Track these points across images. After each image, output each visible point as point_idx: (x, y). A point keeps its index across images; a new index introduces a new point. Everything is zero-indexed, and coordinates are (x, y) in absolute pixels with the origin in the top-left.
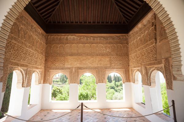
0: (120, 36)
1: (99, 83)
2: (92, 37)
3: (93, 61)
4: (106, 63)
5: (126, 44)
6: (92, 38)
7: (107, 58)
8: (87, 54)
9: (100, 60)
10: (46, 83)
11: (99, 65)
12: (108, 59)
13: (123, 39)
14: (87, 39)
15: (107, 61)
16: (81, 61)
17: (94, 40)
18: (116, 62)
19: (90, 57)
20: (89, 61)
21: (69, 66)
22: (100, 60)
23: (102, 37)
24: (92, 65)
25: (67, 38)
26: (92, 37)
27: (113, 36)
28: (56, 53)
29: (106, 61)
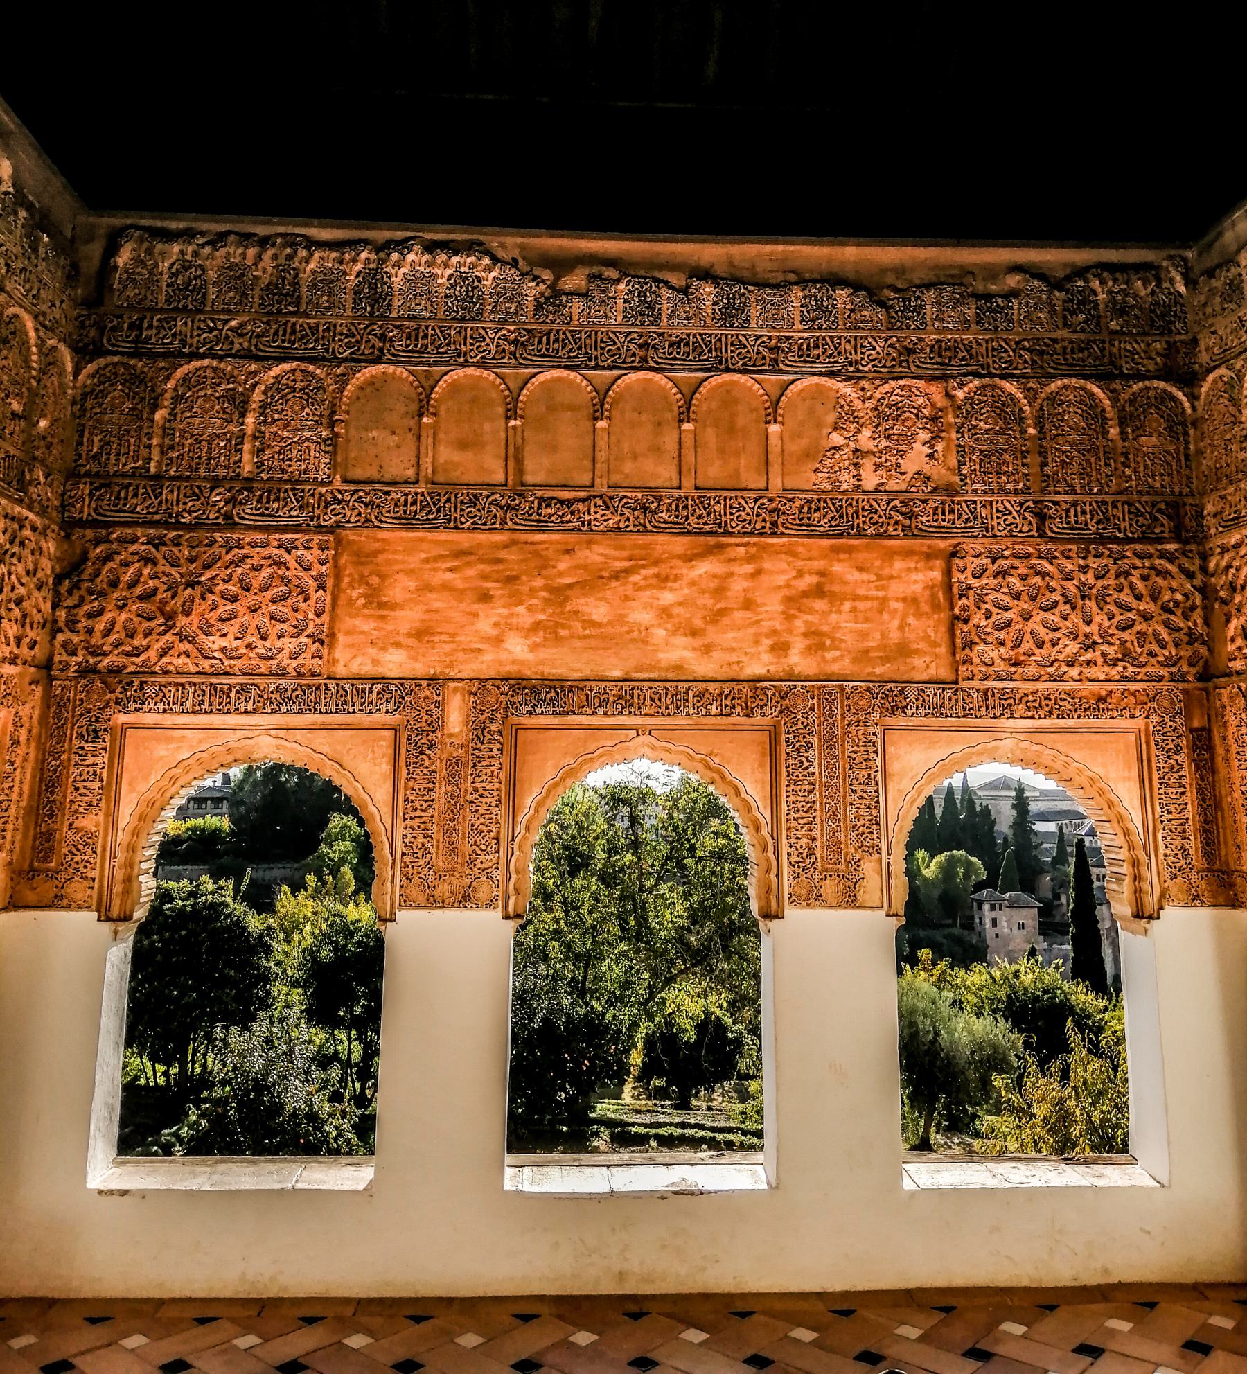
0: (1081, 272)
1: (796, 901)
2: (705, 274)
3: (720, 591)
4: (895, 636)
5: (1166, 374)
6: (709, 288)
7: (899, 565)
8: (646, 511)
9: (818, 591)
10: (57, 901)
11: (798, 660)
12: (919, 578)
13: (1120, 311)
14: (650, 309)
15: (912, 601)
16: (559, 595)
17: (730, 313)
18: (1027, 617)
19: (680, 544)
20: (667, 597)
21: (395, 663)
22: (818, 591)
23: (835, 280)
24: (707, 649)
25: (374, 281)
26: (705, 274)
27: (992, 273)
28: (216, 483)
29: (885, 604)
